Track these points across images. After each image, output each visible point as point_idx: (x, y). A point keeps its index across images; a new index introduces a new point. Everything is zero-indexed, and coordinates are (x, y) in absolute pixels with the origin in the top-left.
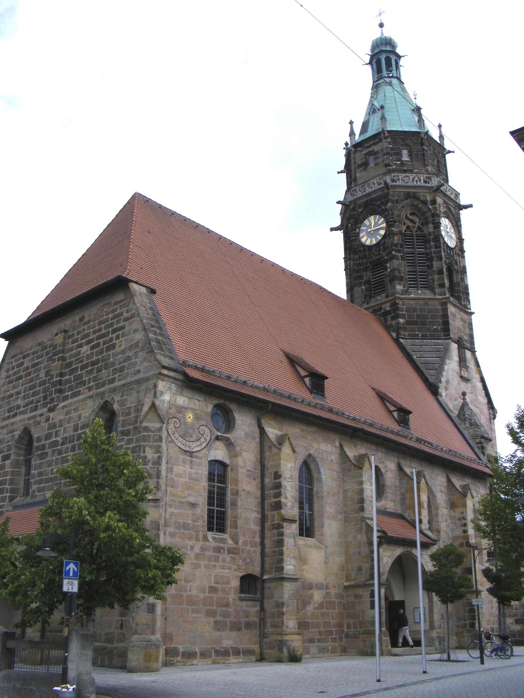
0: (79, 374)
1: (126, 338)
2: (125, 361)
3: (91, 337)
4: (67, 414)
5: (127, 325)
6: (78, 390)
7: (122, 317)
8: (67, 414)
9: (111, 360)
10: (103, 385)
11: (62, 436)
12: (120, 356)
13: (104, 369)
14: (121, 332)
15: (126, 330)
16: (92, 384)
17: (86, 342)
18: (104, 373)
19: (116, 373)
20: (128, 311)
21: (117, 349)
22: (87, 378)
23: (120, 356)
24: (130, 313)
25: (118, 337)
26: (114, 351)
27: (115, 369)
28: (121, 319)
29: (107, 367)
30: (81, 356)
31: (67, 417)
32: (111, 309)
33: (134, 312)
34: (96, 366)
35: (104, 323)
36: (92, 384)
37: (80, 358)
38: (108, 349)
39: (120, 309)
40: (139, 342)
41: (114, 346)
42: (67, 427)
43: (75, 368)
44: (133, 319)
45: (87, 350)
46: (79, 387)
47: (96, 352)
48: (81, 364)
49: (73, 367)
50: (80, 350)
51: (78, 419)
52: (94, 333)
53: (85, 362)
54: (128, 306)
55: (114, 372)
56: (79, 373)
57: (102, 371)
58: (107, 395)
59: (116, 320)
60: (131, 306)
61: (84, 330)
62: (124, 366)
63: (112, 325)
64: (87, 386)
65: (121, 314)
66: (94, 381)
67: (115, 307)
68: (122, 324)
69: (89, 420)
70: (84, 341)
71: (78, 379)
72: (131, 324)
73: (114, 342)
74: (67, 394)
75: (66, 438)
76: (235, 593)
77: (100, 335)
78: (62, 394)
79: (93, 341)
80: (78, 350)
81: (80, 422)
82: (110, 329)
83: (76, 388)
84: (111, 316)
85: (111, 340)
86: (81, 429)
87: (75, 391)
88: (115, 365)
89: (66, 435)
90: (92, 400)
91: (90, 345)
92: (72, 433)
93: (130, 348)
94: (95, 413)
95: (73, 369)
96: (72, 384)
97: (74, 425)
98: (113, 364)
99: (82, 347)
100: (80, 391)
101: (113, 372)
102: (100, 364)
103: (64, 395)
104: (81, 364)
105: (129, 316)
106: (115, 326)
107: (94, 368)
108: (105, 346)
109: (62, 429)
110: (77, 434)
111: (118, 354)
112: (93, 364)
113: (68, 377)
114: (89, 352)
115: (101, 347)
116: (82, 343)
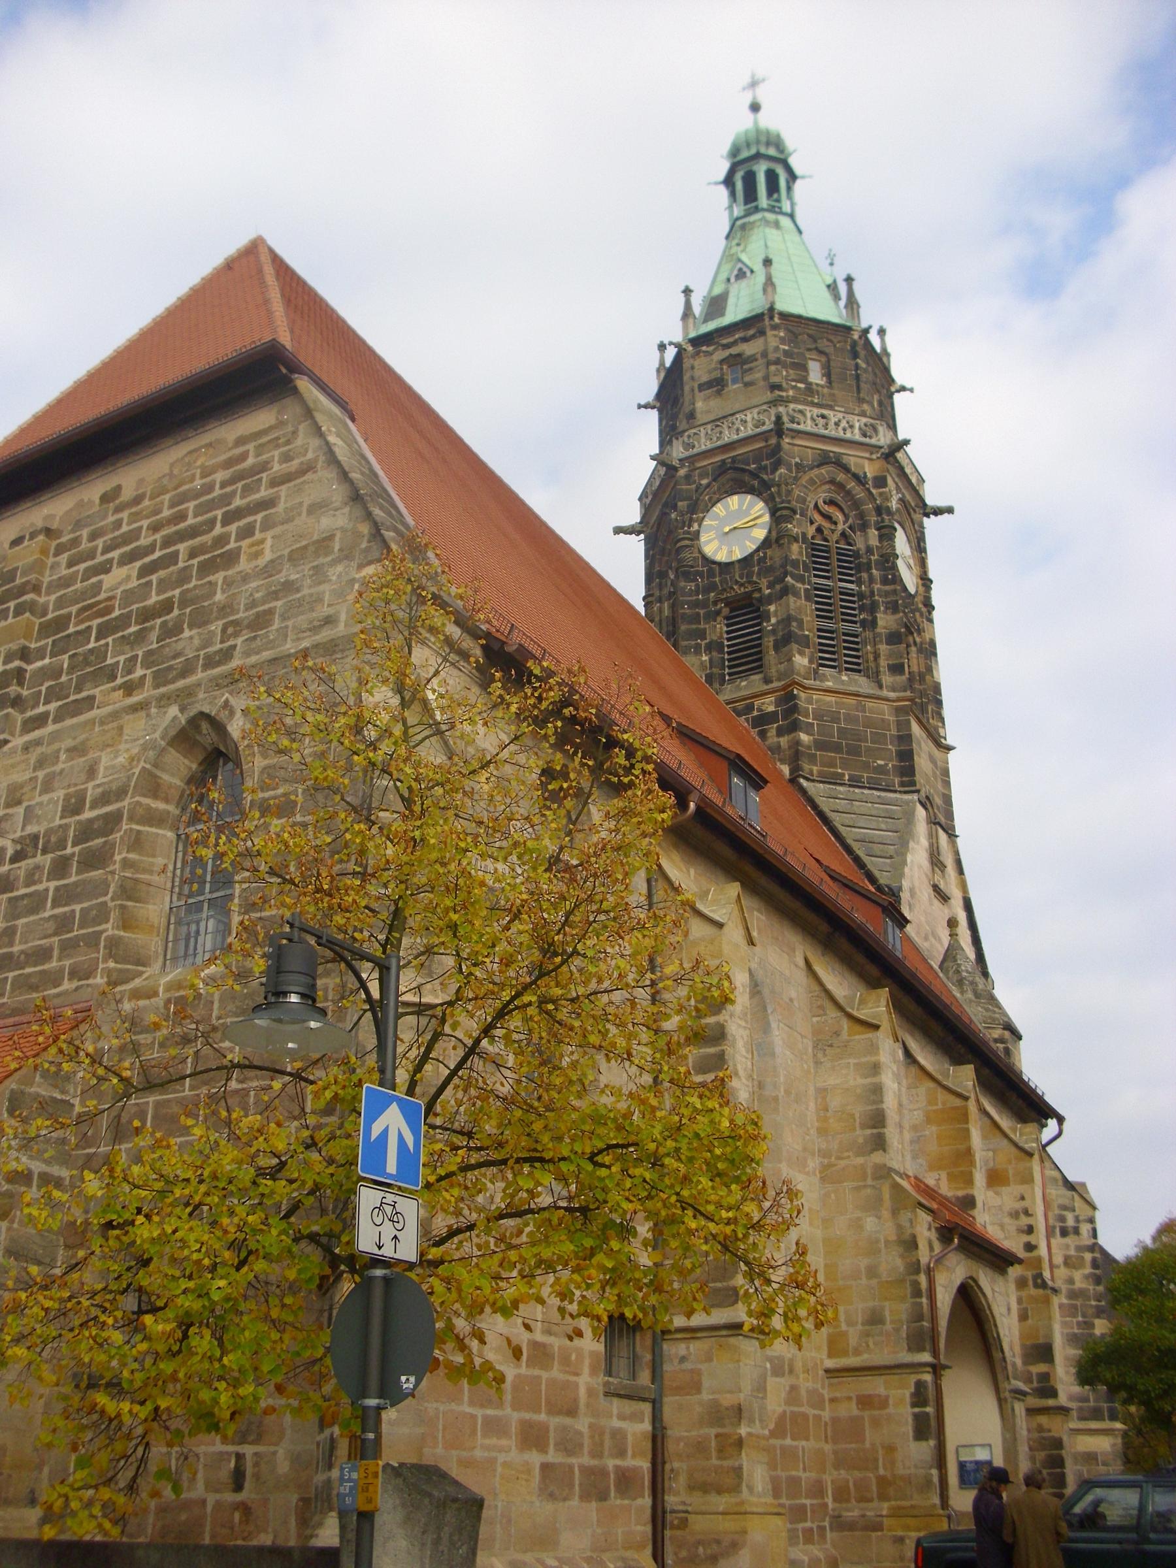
0: (91, 651)
1: (278, 530)
2: (274, 595)
3: (144, 541)
4: (40, 764)
5: (283, 494)
6: (84, 694)
7: (264, 475)
8: (40, 764)
9: (219, 597)
10: (186, 671)
11: (19, 834)
12: (254, 585)
13: (191, 627)
14: (259, 517)
15: (281, 507)
16: (139, 672)
17: (122, 556)
18: (191, 638)
19: (236, 635)
20: (286, 458)
21: (244, 565)
22: (122, 658)
23: (254, 585)
24: (296, 462)
25: (247, 532)
26: (230, 572)
27: (235, 623)
28: (260, 480)
29: (199, 620)
30: (103, 596)
31: (41, 774)
32: (223, 457)
33: (310, 455)
34: (159, 621)
35: (197, 497)
36: (139, 672)
37: (99, 602)
38: (207, 568)
39: (257, 456)
40: (331, 538)
41: (231, 558)
42: (41, 804)
43: (78, 633)
44: (309, 476)
45: (128, 578)
46: (88, 685)
47: (161, 581)
48: (99, 620)
49: (71, 630)
50: (100, 582)
51: (83, 777)
52: (155, 528)
53: (116, 613)
54: (288, 442)
55: (230, 630)
56: (92, 645)
57: (182, 631)
58: (201, 695)
59: (240, 485)
60: (299, 442)
61: (118, 524)
62: (271, 612)
63: (226, 499)
64: (119, 681)
65: (264, 467)
66: (146, 665)
67: (241, 449)
68: (263, 493)
69: (129, 778)
70: (115, 554)
71: (87, 663)
72: (299, 490)
73: (232, 545)
74: (41, 709)
75: (35, 838)
76: (594, 1371)
77: (177, 533)
78: (23, 712)
79: (153, 551)
80: (94, 580)
81: (90, 785)
82: (219, 513)
83: (79, 689)
84: (220, 476)
85: (222, 540)
86: (92, 808)
87: (72, 698)
88: (234, 611)
89: (31, 829)
90: (143, 714)
91: (138, 564)
92: (58, 822)
93: (295, 557)
94: (151, 754)
95: (69, 636)
96: (64, 678)
97: (67, 798)
98: (226, 609)
99: (107, 571)
100: (92, 698)
101: (224, 630)
102: (176, 612)
103: (29, 714)
104: (99, 620)
105: (293, 469)
106: (238, 502)
107: (153, 628)
108: (195, 562)
109: (20, 810)
110: (79, 822)
111: (245, 578)
112: (147, 615)
113: (47, 661)
114: (134, 583)
115: (181, 564)
116: (111, 561)
